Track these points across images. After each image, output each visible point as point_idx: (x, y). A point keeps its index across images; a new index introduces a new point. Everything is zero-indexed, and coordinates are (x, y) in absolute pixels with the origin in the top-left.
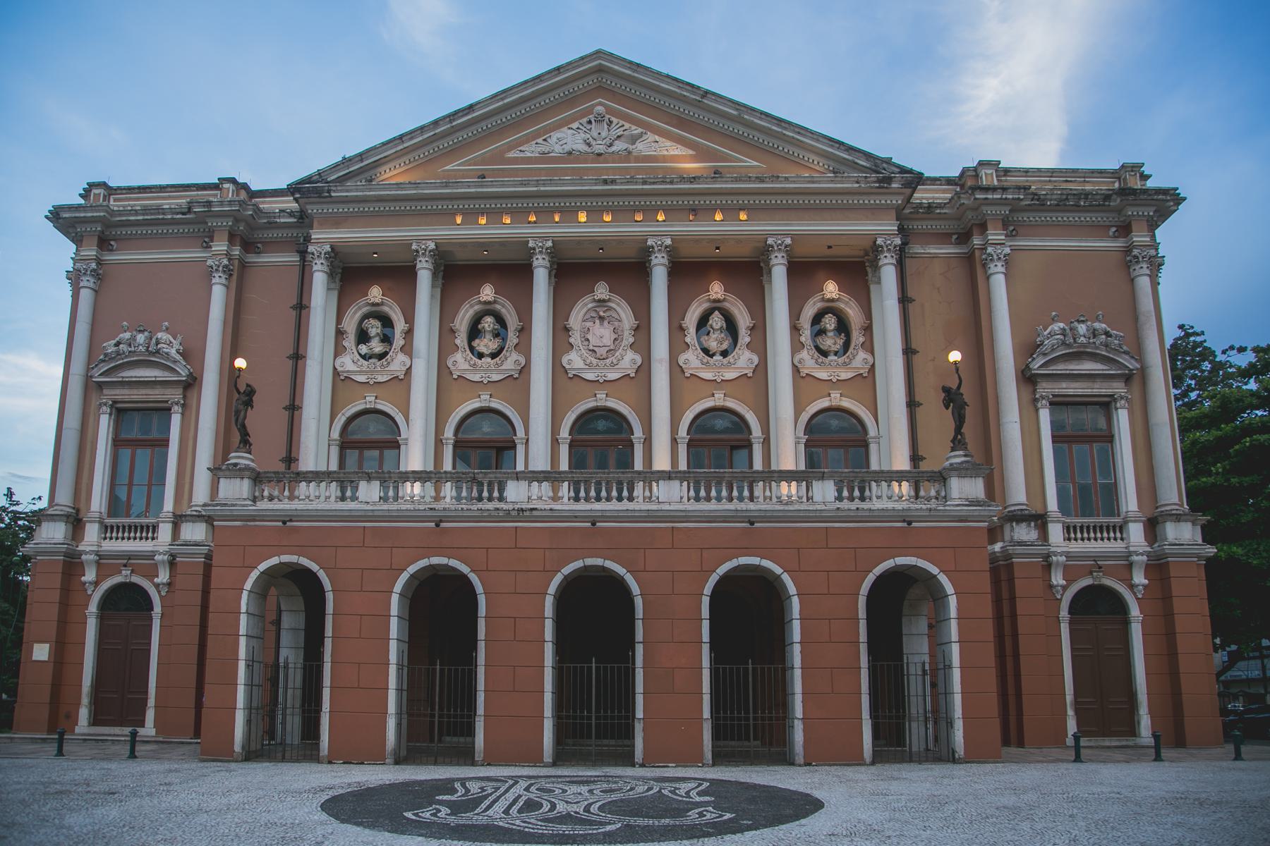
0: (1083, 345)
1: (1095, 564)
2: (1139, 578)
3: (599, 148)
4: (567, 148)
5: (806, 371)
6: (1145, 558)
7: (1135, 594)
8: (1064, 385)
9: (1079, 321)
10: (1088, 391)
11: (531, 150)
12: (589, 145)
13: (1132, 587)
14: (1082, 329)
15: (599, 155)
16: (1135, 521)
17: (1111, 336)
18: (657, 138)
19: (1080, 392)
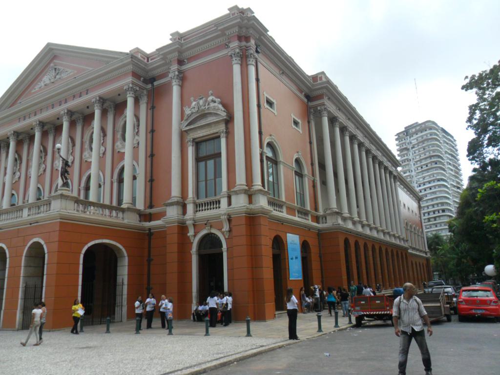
0: (203, 110)
1: (208, 223)
2: (226, 228)
3: (52, 80)
4: (45, 83)
5: (118, 150)
6: (226, 217)
7: (224, 236)
8: (199, 132)
9: (200, 99)
10: (209, 133)
11: (37, 88)
12: (50, 80)
13: (223, 233)
14: (201, 102)
15: (53, 83)
16: (223, 197)
17: (215, 102)
18: (68, 70)
19: (205, 134)
